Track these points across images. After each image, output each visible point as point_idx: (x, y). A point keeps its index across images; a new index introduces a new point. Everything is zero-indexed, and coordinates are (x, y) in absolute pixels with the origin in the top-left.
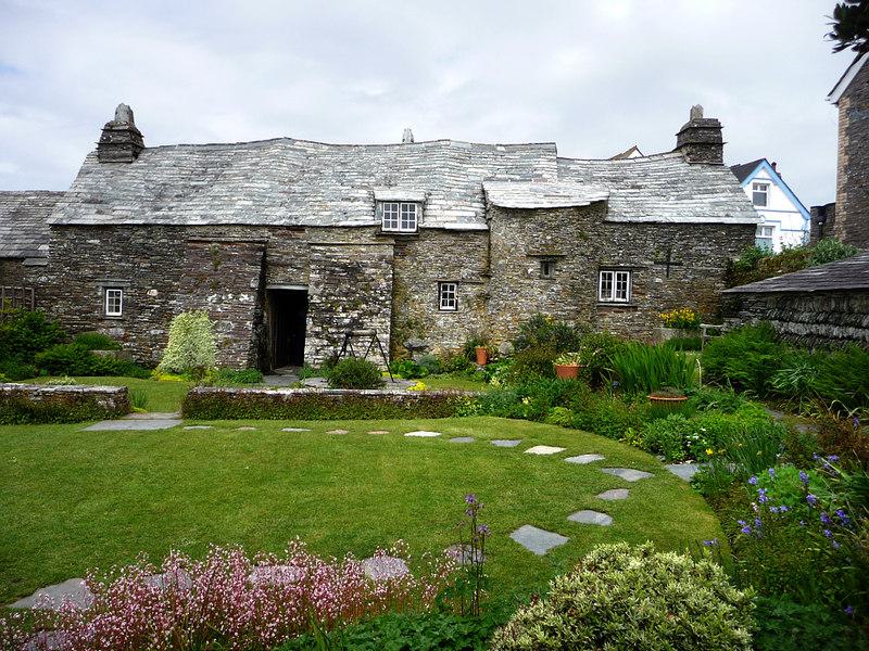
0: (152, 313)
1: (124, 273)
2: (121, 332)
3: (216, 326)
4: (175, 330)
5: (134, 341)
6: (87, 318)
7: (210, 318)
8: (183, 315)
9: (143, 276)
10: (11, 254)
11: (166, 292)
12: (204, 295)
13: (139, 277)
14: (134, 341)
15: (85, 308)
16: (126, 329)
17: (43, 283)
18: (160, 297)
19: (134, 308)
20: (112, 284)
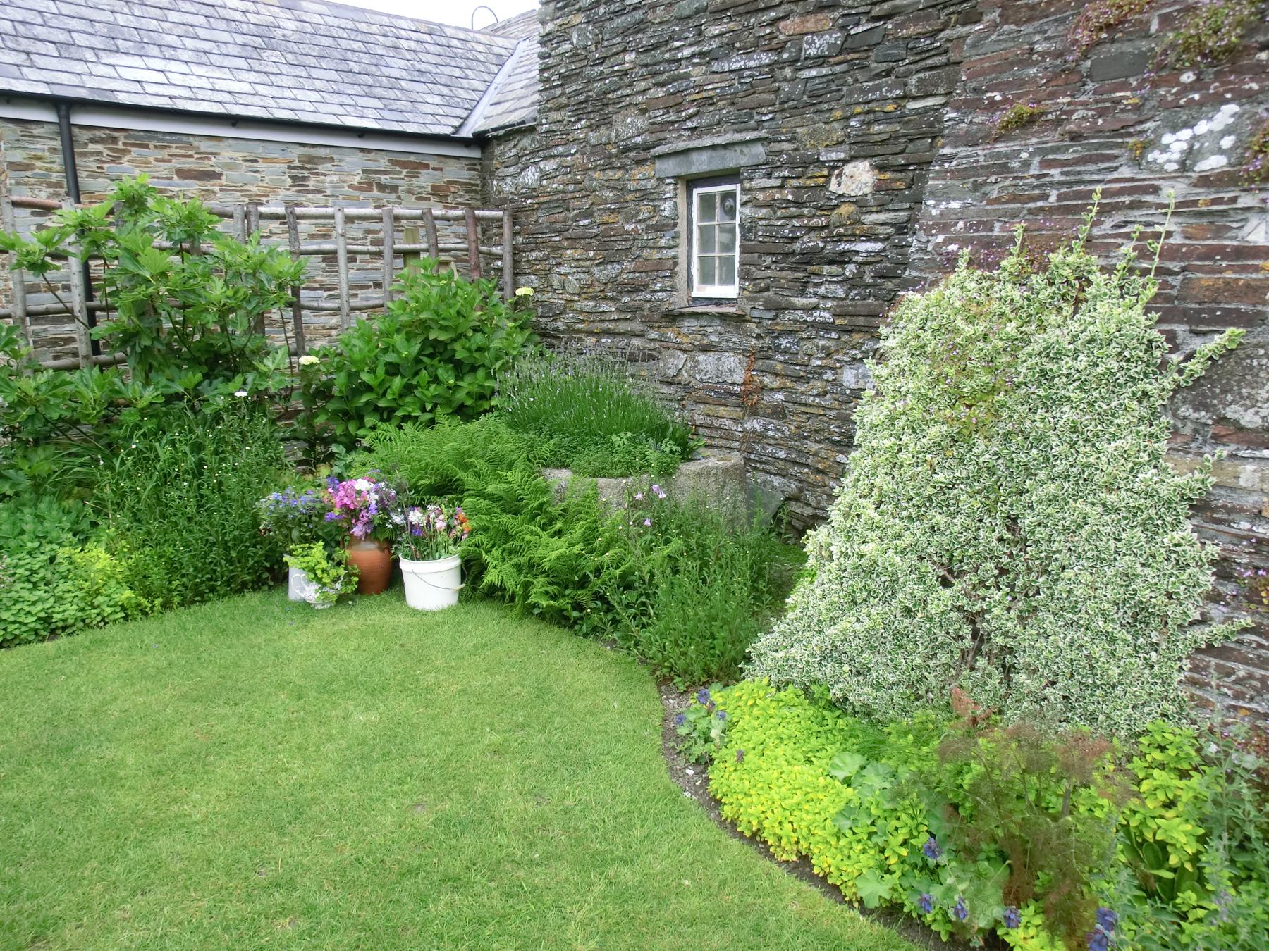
0: (852, 283)
1: (742, 104)
2: (732, 368)
3: (1224, 375)
4: (891, 387)
5: (778, 413)
6: (636, 310)
7: (1168, 309)
8: (961, 284)
9: (815, 98)
10: (514, 118)
11: (906, 162)
12: (1121, 134)
13: (798, 109)
14: (778, 413)
15: (625, 271)
16: (752, 356)
17: (532, 192)
18: (885, 195)
19: (784, 258)
20: (701, 163)
